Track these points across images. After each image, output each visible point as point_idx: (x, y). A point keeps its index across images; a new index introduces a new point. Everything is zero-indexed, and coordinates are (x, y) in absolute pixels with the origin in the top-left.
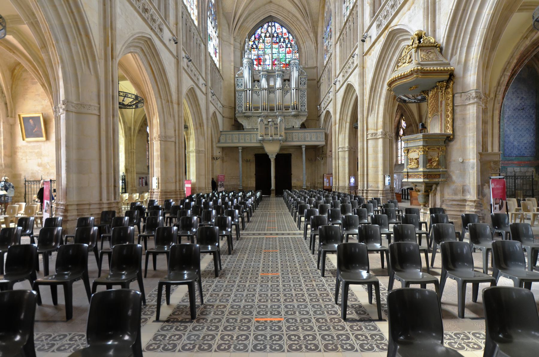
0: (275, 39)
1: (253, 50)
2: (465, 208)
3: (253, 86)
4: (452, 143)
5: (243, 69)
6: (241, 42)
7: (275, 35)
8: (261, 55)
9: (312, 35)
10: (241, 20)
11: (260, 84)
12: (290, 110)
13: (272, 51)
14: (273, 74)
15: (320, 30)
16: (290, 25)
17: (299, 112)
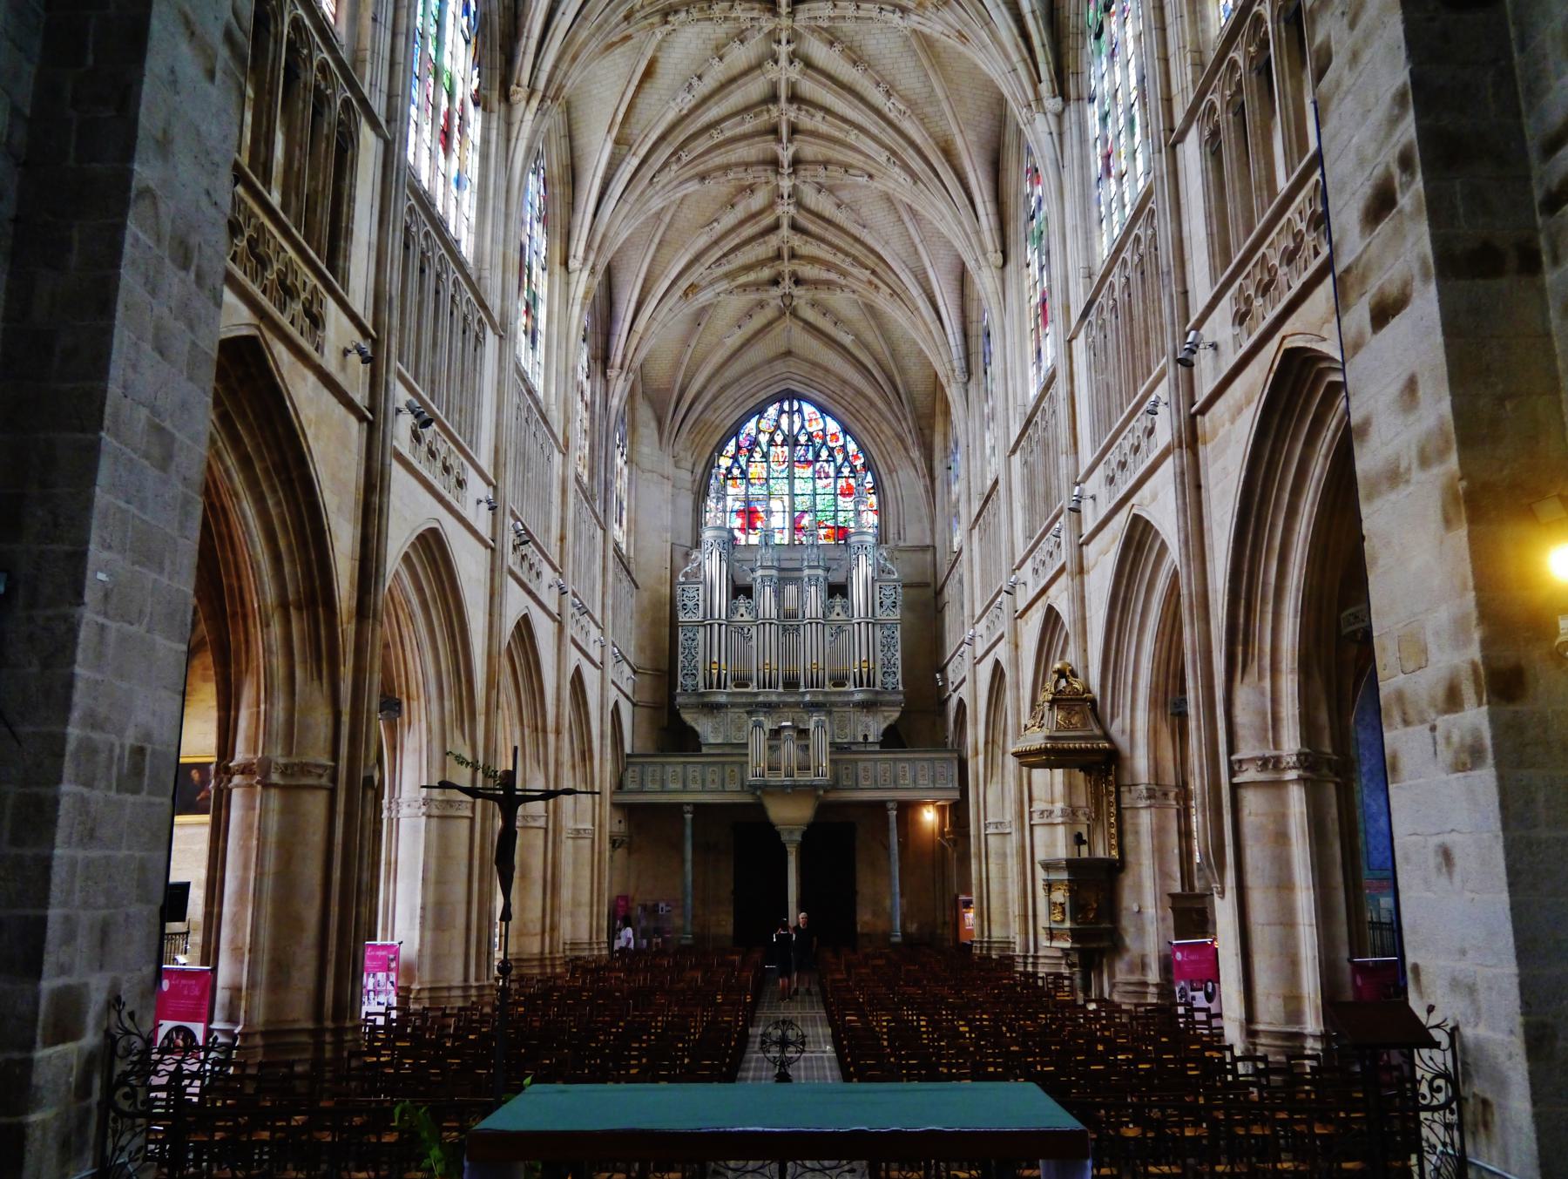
0: (800, 451)
1: (730, 482)
2: (1145, 998)
3: (732, 610)
4: (1122, 875)
6: (694, 465)
7: (803, 439)
8: (758, 500)
9: (915, 454)
10: (699, 407)
11: (753, 603)
12: (850, 687)
13: (792, 486)
14: (796, 574)
17: (877, 693)
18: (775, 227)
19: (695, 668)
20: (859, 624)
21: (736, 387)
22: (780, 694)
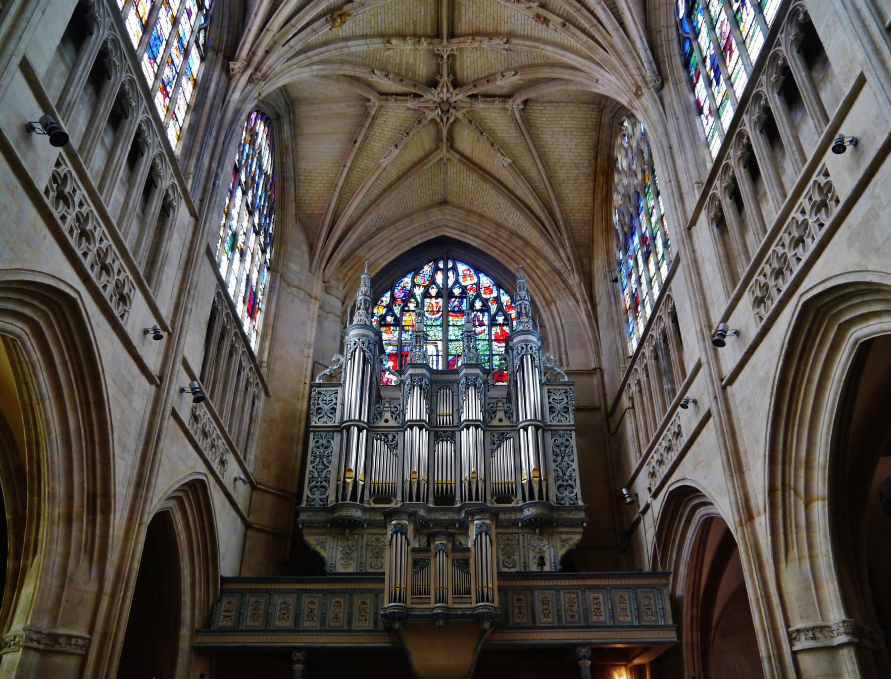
1: (383, 329)
5: (342, 359)
6: (345, 297)
7: (457, 292)
9: (574, 280)
10: (353, 237)
12: (517, 502)
13: (446, 332)
15: (599, 264)
17: (552, 509)
19: (327, 479)
20: (526, 429)
22: (429, 510)
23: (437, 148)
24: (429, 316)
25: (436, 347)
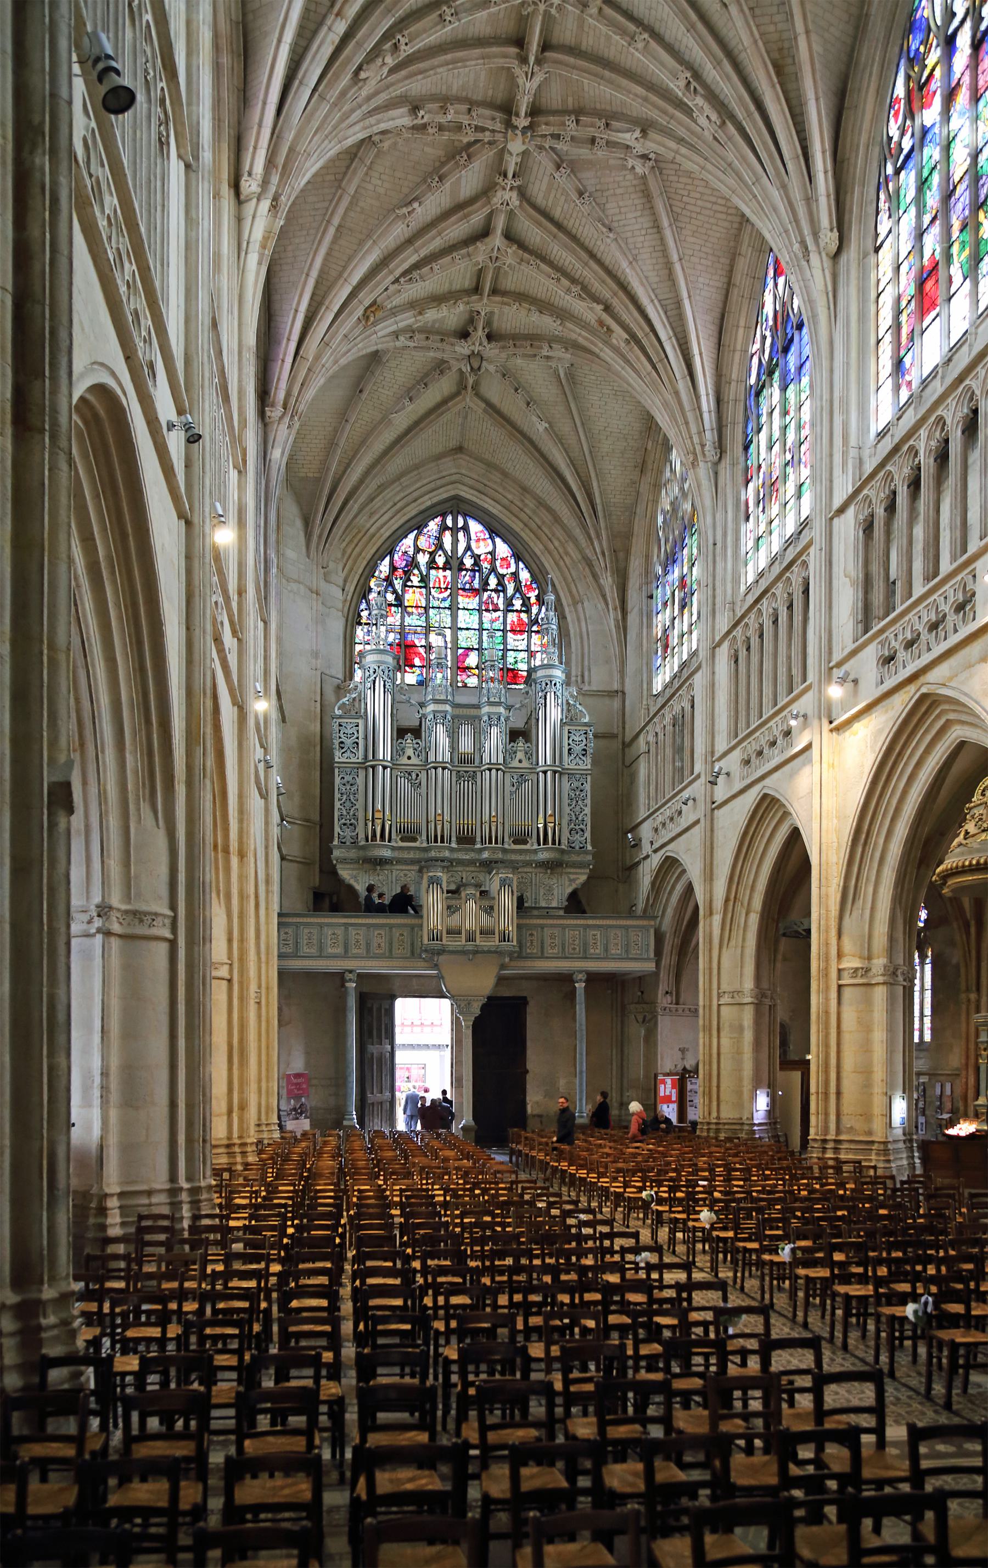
0: (465, 577)
7: (468, 562)
9: (608, 581)
10: (354, 506)
12: (532, 845)
13: (454, 618)
14: (473, 712)
15: (635, 566)
16: (526, 535)
17: (563, 851)
18: (485, 233)
20: (545, 772)
21: (396, 487)
23: (458, 393)
24: (436, 595)
25: (445, 636)
